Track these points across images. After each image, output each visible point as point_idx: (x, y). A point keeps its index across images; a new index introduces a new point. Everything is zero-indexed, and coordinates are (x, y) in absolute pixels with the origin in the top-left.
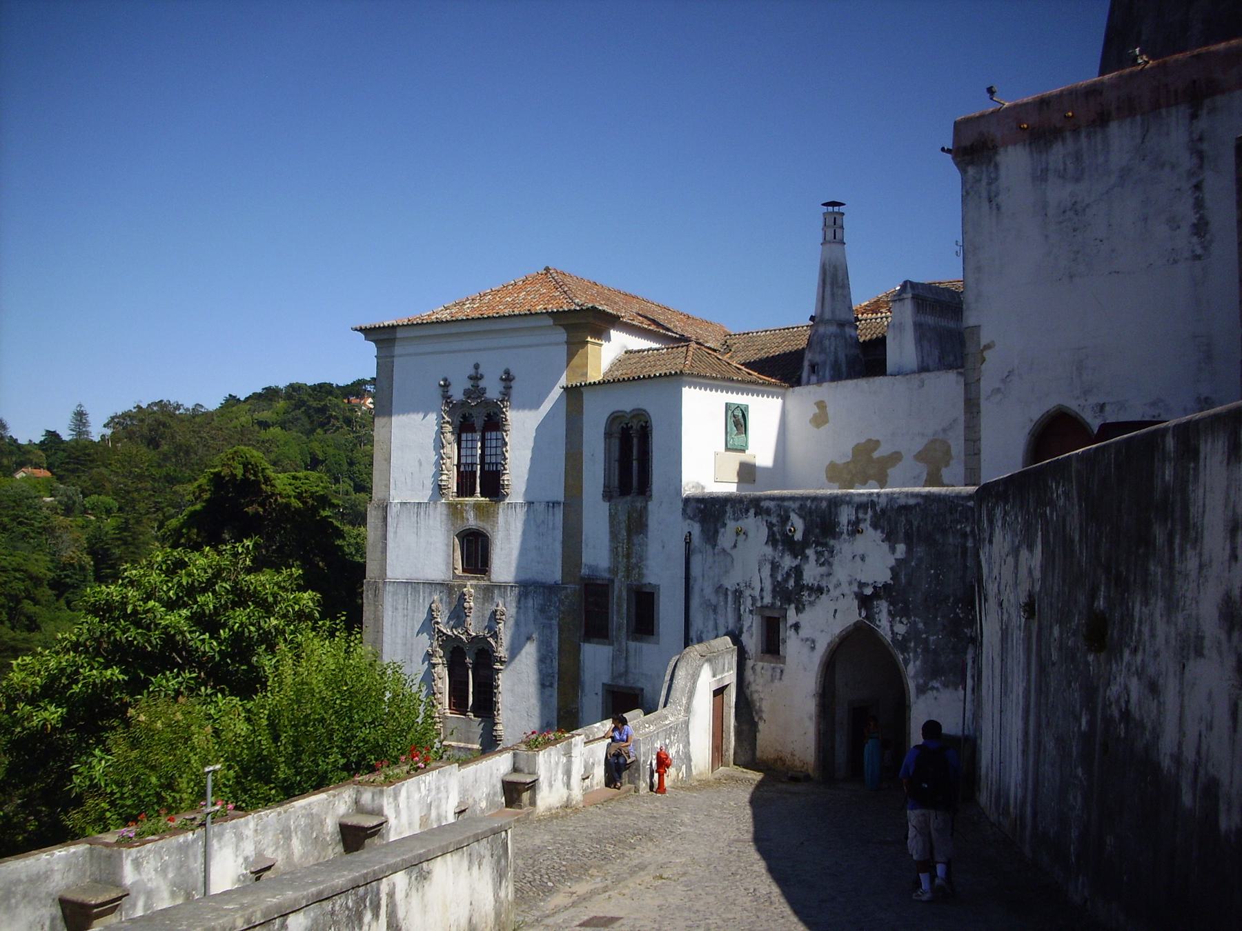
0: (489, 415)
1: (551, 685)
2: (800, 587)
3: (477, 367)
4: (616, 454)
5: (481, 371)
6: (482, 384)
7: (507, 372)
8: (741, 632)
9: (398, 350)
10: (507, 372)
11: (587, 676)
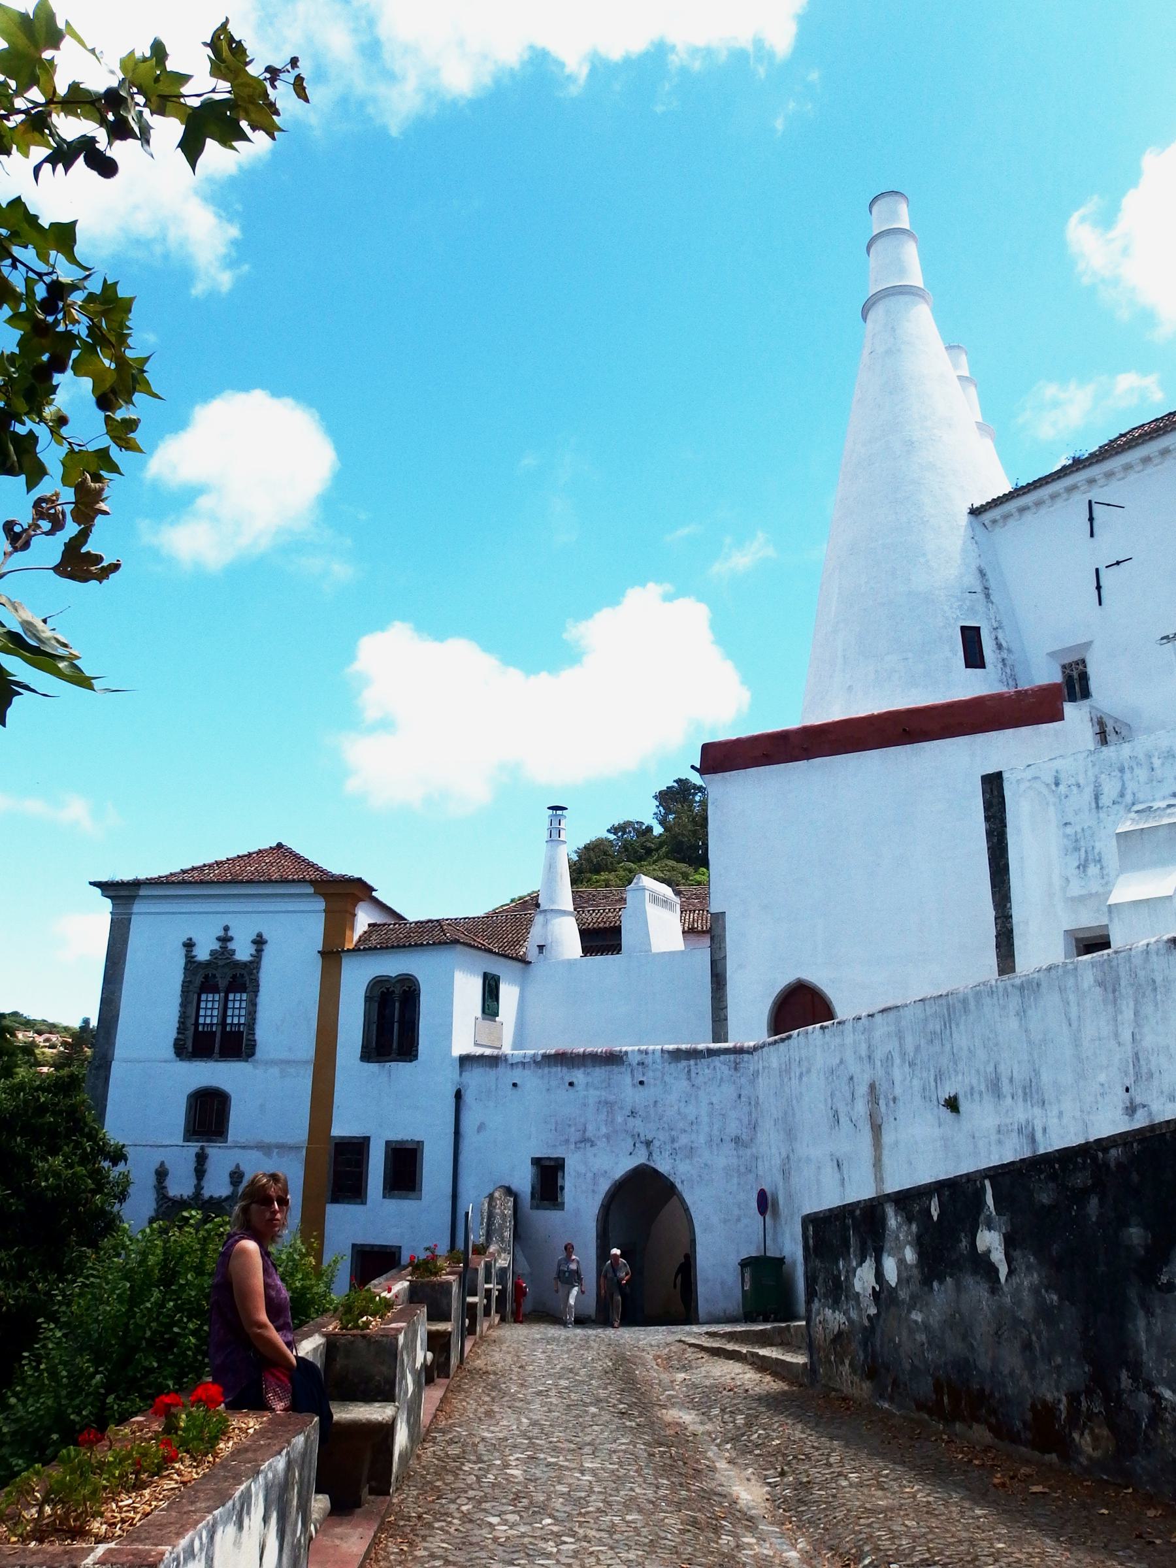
3: (226, 929)
5: (230, 933)
6: (231, 946)
7: (260, 935)
9: (138, 907)
10: (260, 935)
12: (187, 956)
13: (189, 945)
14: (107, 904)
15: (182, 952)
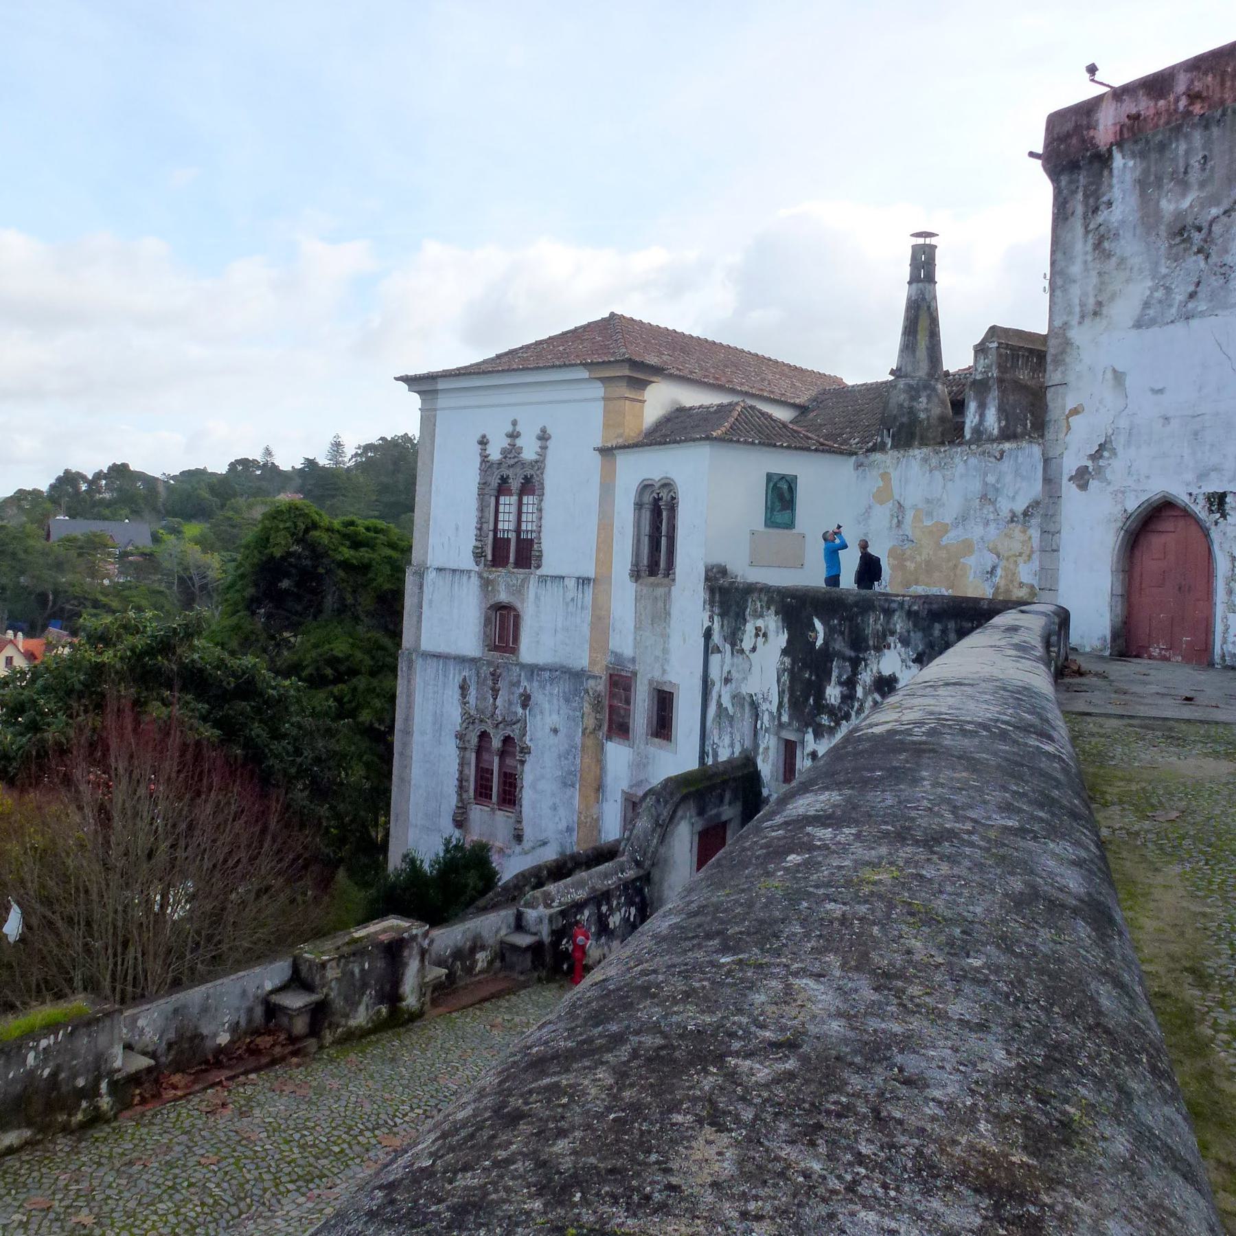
0: (526, 478)
1: (573, 786)
2: (821, 706)
3: (514, 423)
4: (646, 528)
5: (518, 428)
6: (519, 442)
7: (544, 430)
8: (757, 753)
11: (609, 780)
13: (483, 442)
14: (415, 400)
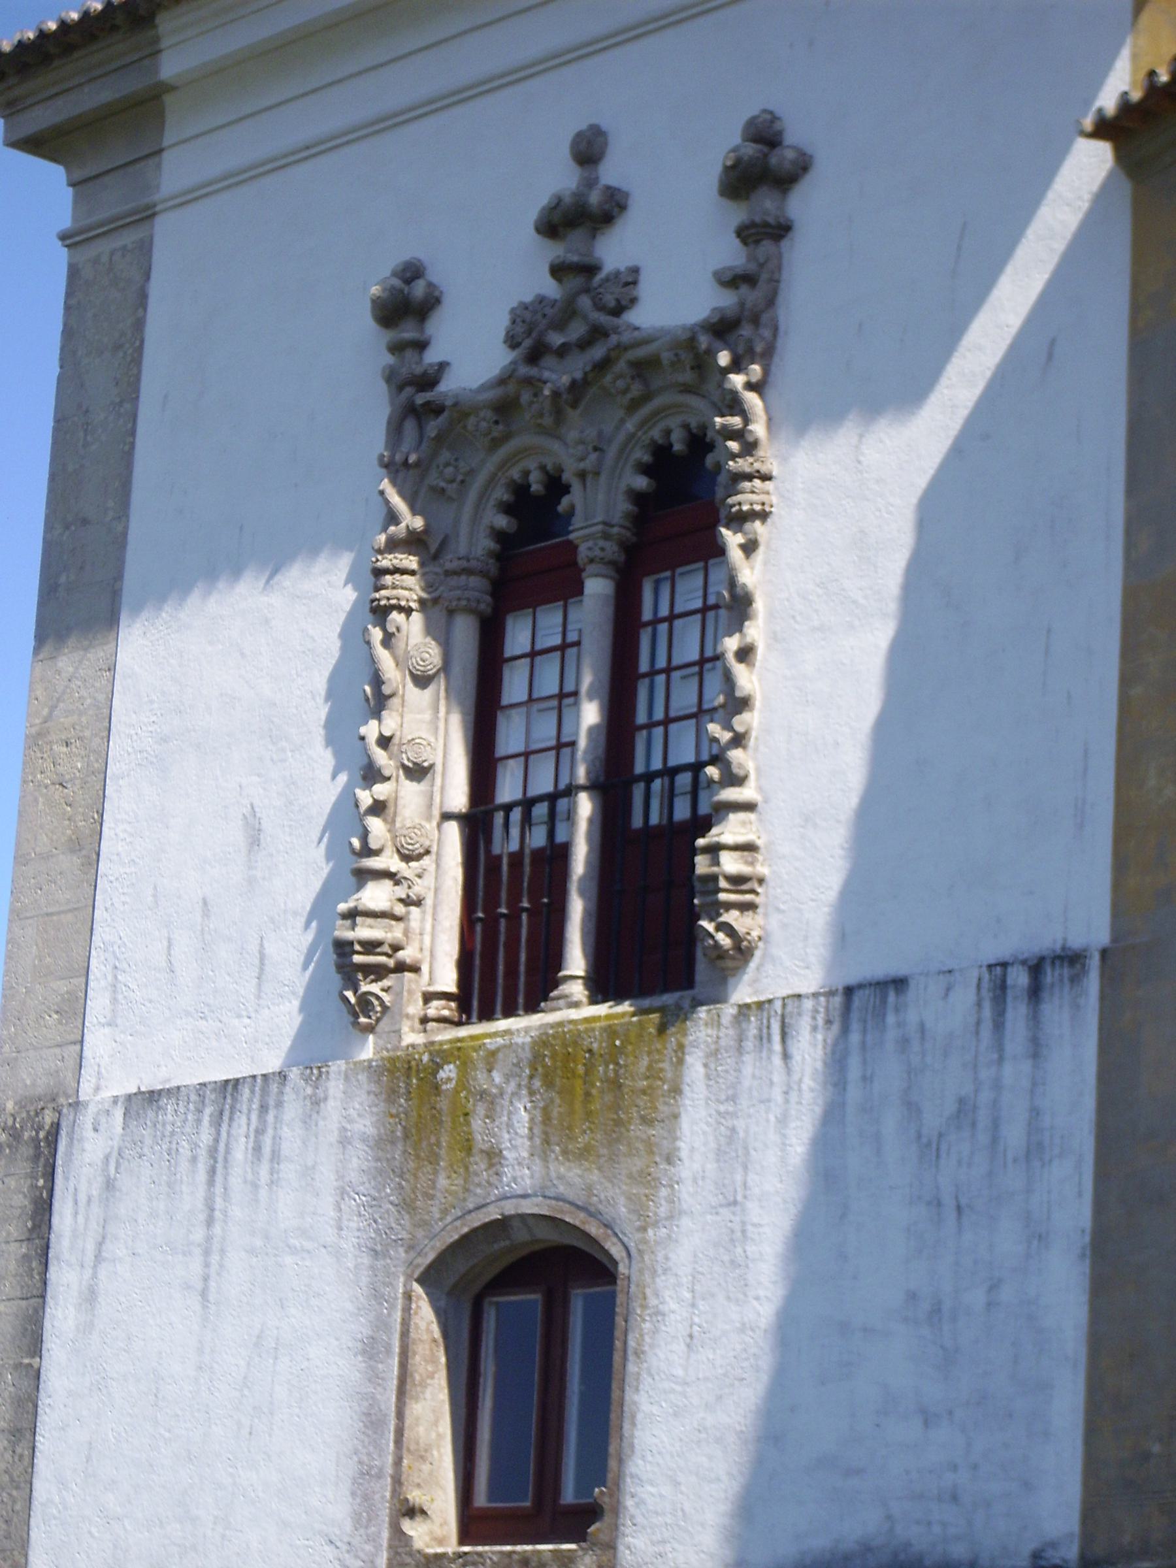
3: (588, 150)
5: (610, 173)
6: (614, 251)
7: (765, 133)
9: (176, 171)
10: (765, 133)
12: (397, 381)
13: (406, 307)
15: (364, 349)
